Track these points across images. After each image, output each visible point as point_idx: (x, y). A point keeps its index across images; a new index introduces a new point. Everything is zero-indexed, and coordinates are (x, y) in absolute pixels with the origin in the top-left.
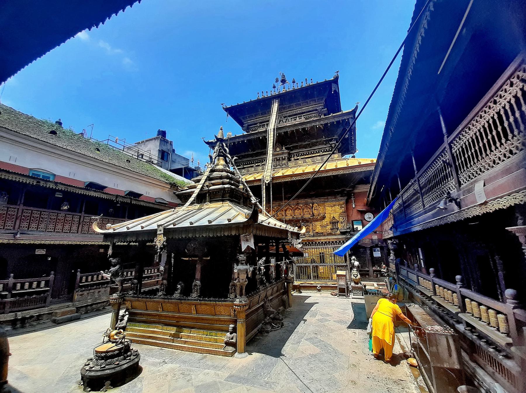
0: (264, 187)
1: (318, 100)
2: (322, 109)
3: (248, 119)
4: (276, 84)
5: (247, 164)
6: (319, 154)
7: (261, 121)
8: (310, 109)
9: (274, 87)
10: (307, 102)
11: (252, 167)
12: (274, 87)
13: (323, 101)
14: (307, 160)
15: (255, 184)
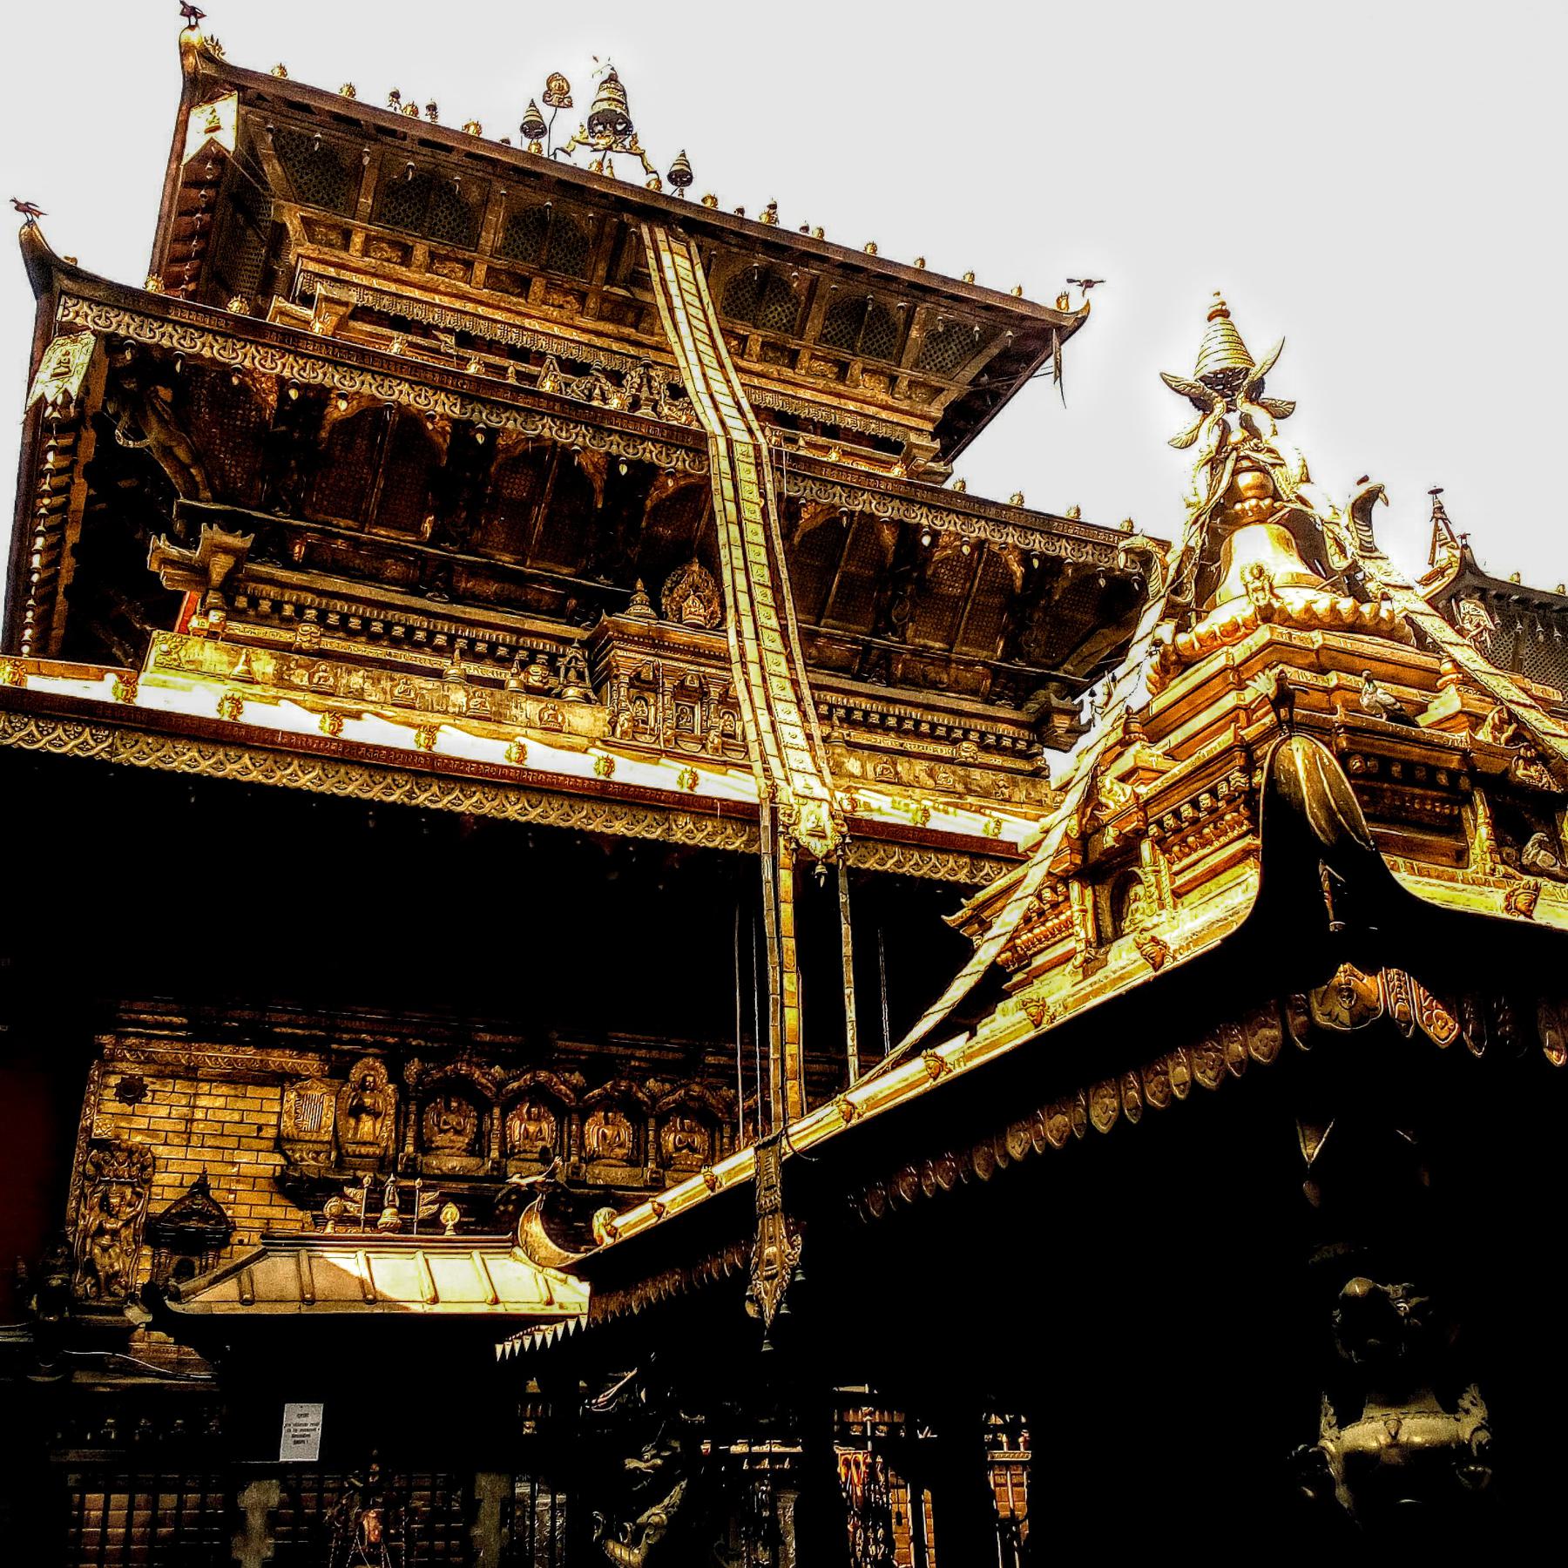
0: (786, 878)
1: (911, 384)
2: (935, 459)
3: (354, 256)
4: (546, 112)
5: (352, 634)
6: (945, 751)
7: (467, 324)
8: (848, 422)
9: (534, 129)
10: (843, 371)
11: (438, 674)
12: (534, 129)
13: (936, 411)
14: (903, 767)
15: (679, 837)
